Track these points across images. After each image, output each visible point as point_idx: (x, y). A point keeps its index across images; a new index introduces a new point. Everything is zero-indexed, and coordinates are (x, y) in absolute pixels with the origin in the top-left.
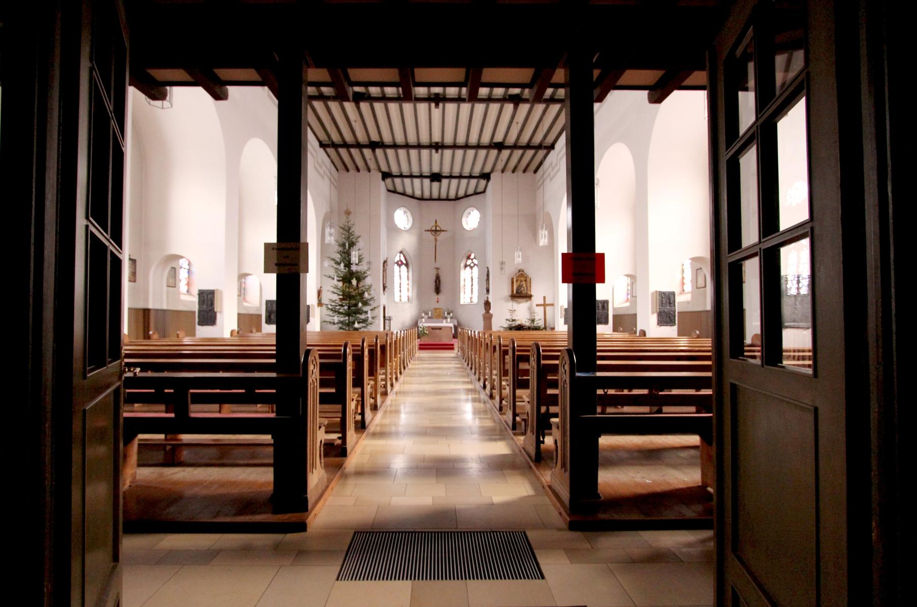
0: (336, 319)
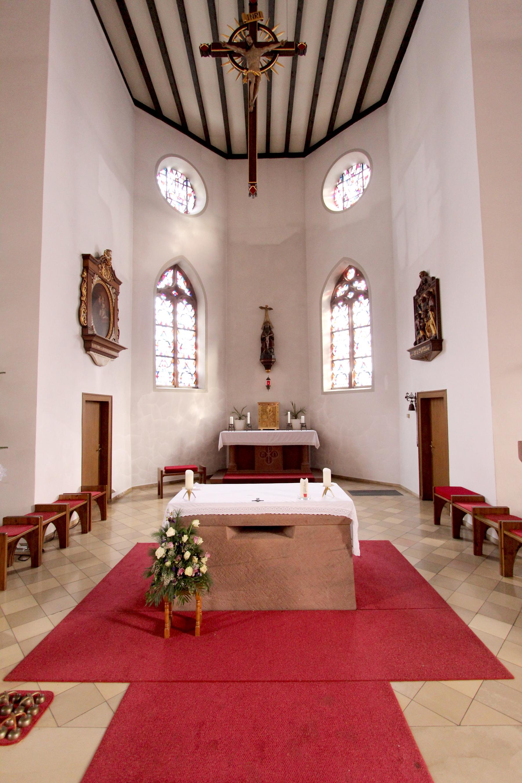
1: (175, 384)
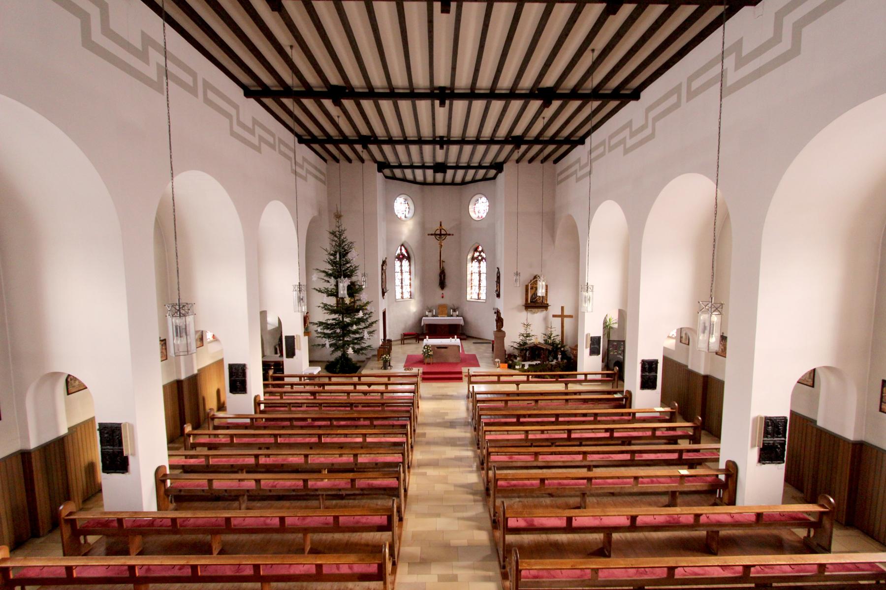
0: (327, 342)
1: (402, 298)
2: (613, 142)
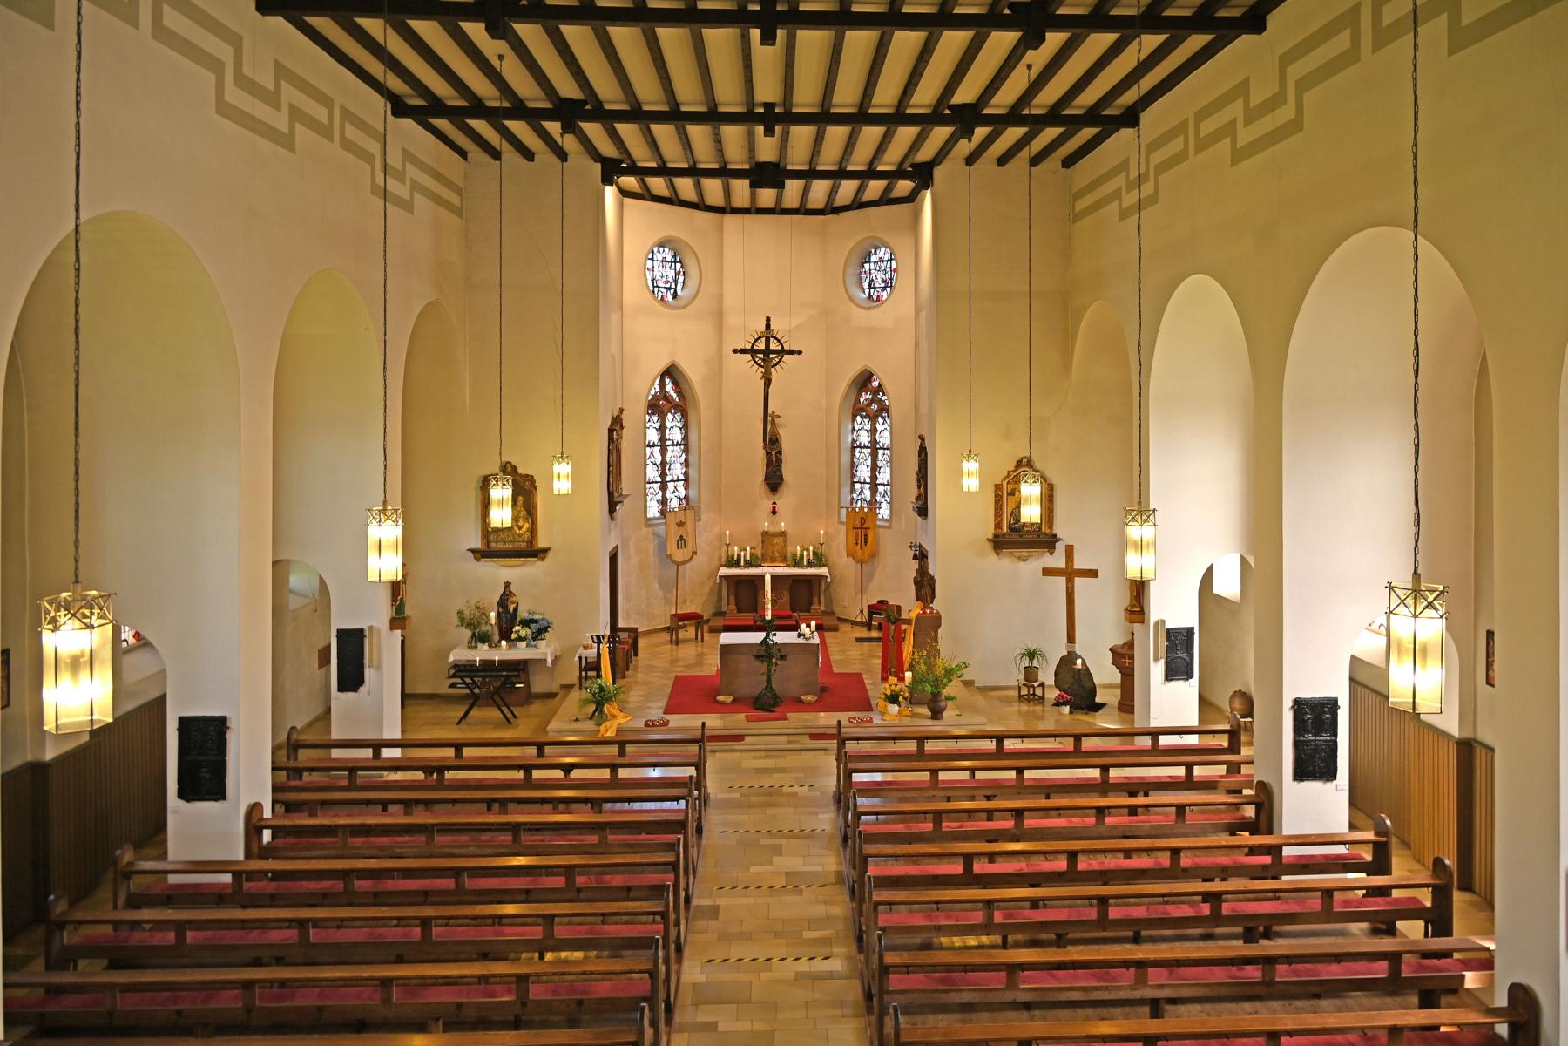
2: (1207, 128)
